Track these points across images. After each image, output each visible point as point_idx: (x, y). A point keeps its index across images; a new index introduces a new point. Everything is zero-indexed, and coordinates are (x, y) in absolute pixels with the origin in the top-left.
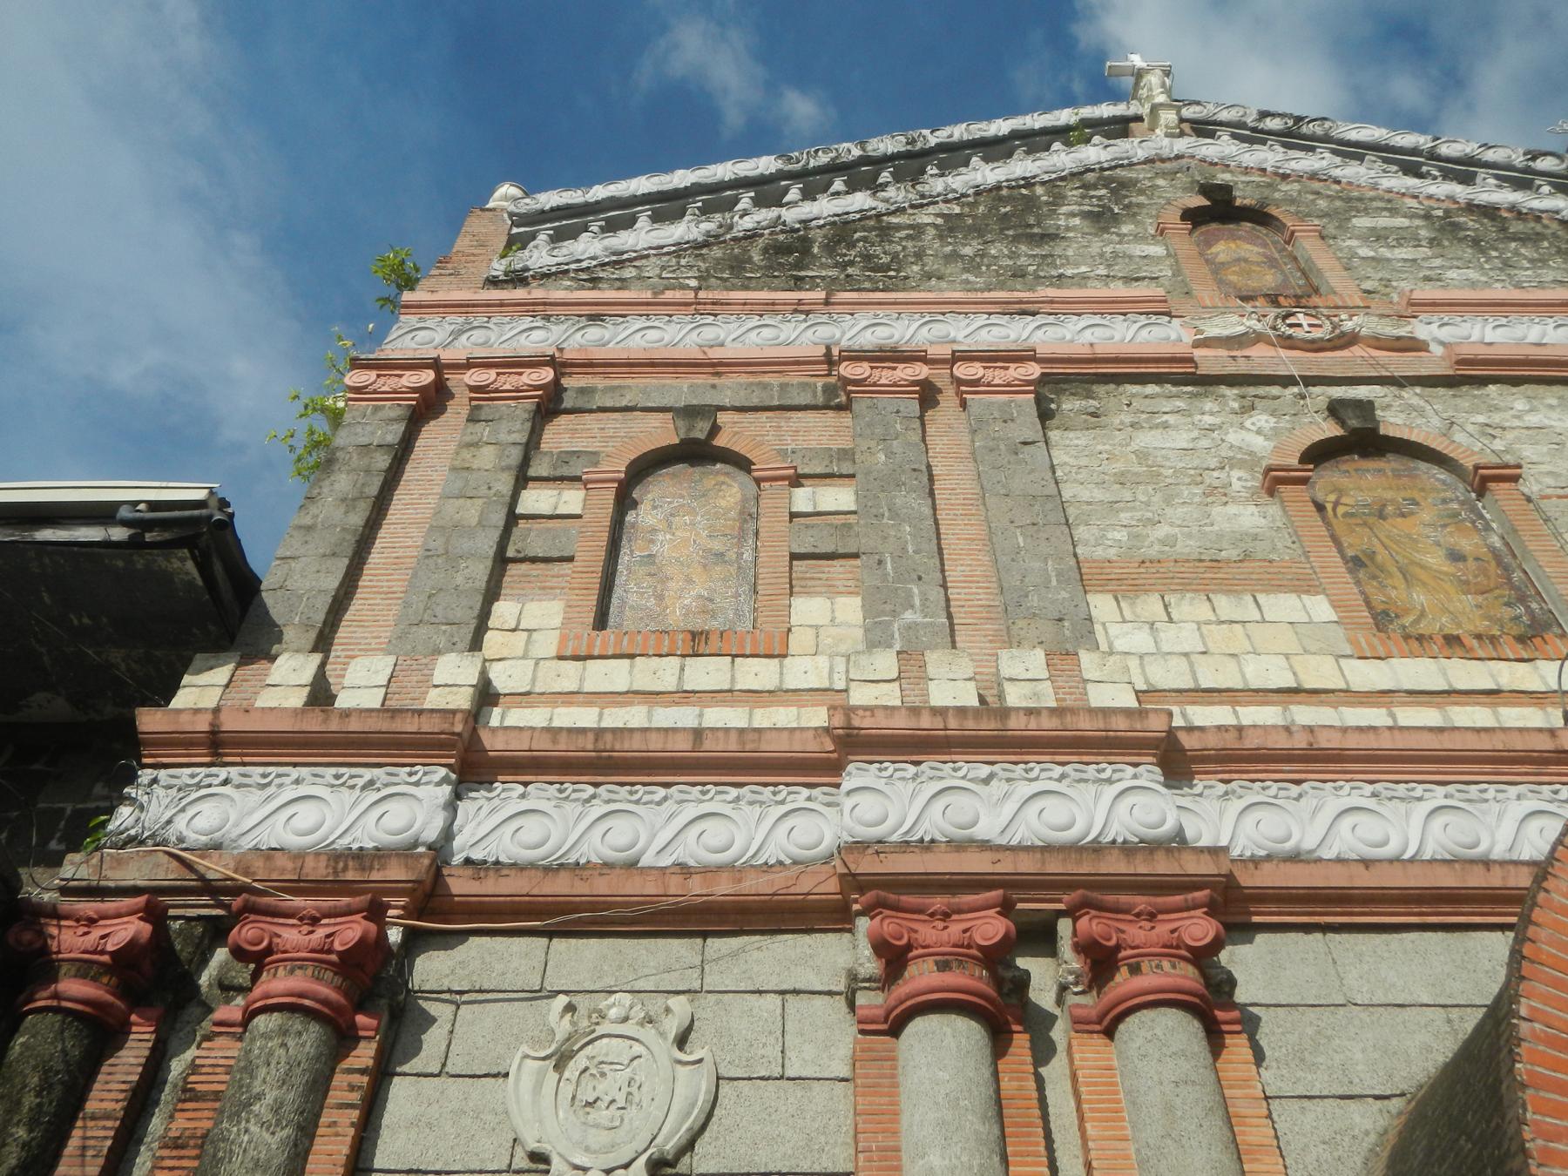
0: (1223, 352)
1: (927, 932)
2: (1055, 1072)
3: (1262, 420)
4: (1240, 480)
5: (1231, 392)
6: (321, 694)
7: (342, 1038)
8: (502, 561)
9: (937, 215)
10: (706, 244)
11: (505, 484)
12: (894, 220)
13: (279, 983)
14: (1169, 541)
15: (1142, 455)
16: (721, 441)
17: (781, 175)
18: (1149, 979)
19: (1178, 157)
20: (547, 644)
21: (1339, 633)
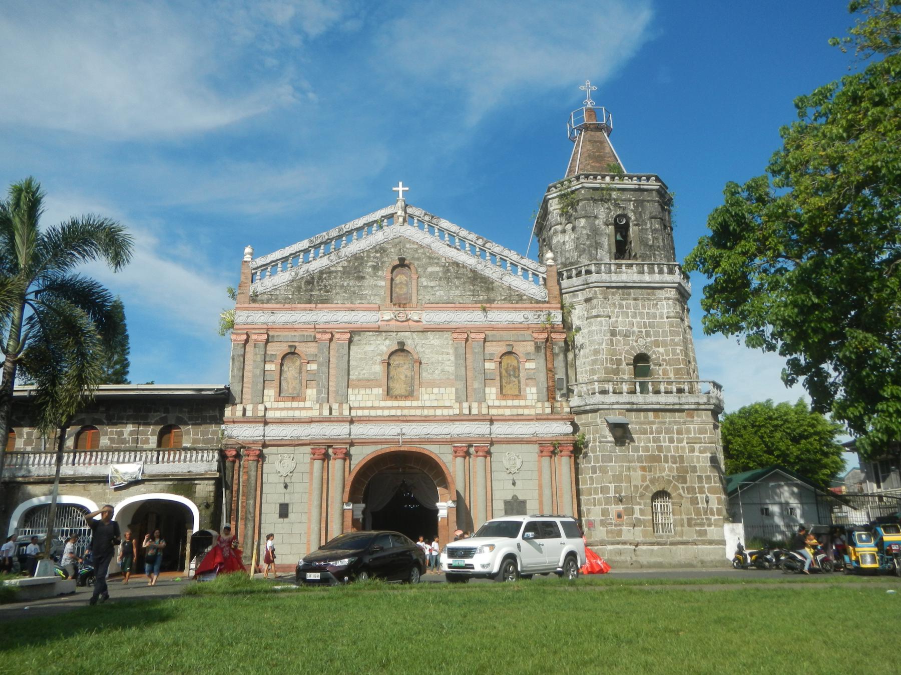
0: (385, 323)
1: (317, 451)
2: (330, 462)
3: (387, 342)
4: (379, 359)
5: (384, 334)
6: (244, 410)
7: (258, 461)
8: (264, 381)
9: (343, 267)
10: (293, 281)
11: (262, 366)
12: (332, 269)
13: (251, 458)
14: (364, 374)
15: (365, 352)
16: (296, 351)
17: (309, 247)
18: (339, 456)
19: (400, 236)
20: (273, 400)
21: (381, 396)
